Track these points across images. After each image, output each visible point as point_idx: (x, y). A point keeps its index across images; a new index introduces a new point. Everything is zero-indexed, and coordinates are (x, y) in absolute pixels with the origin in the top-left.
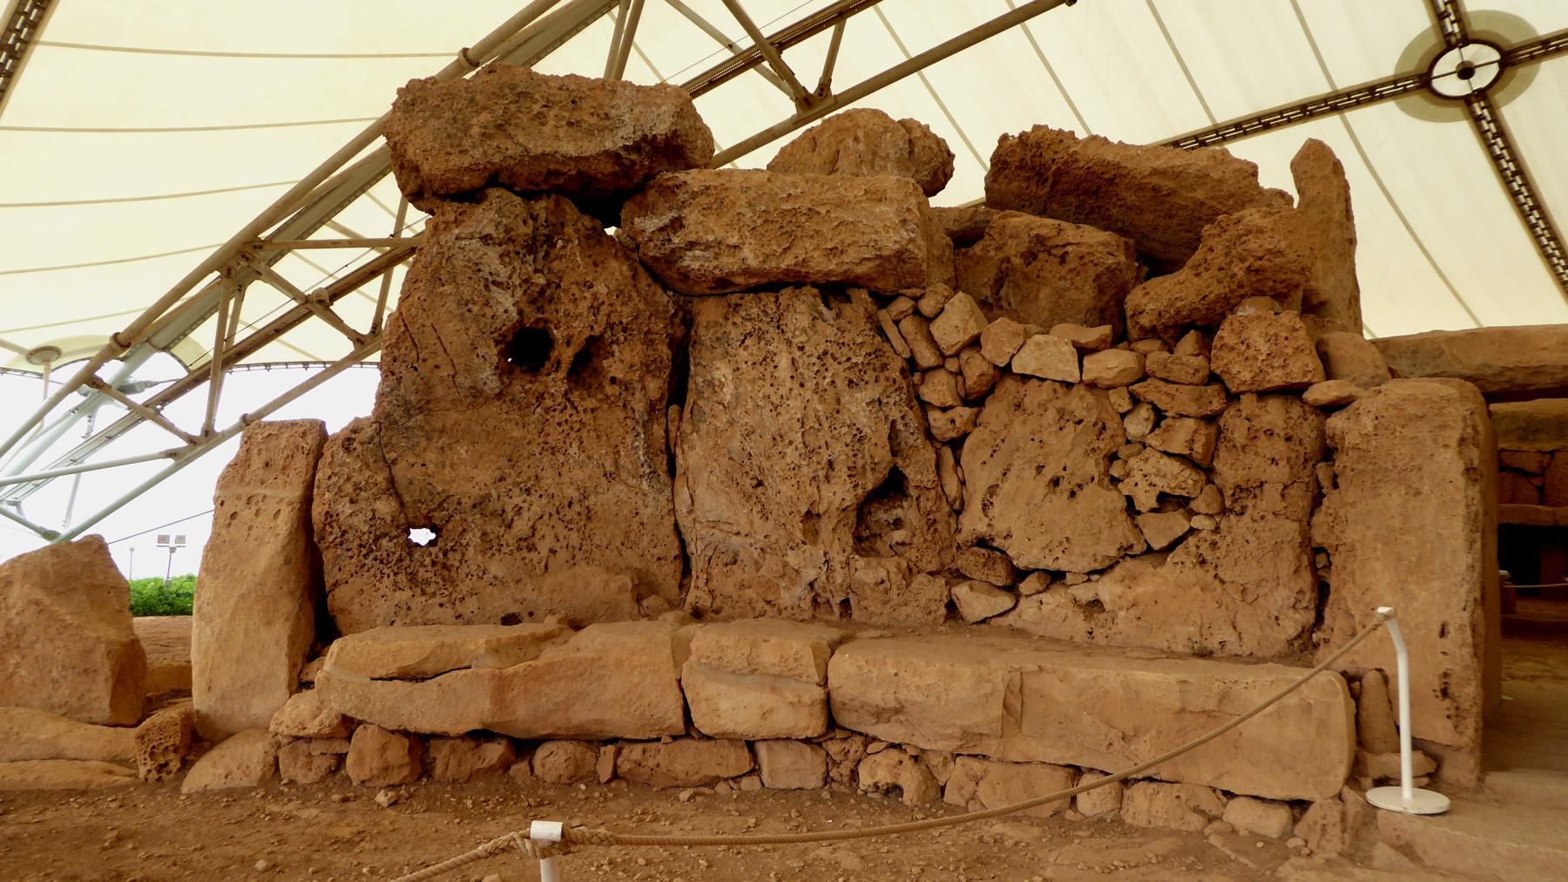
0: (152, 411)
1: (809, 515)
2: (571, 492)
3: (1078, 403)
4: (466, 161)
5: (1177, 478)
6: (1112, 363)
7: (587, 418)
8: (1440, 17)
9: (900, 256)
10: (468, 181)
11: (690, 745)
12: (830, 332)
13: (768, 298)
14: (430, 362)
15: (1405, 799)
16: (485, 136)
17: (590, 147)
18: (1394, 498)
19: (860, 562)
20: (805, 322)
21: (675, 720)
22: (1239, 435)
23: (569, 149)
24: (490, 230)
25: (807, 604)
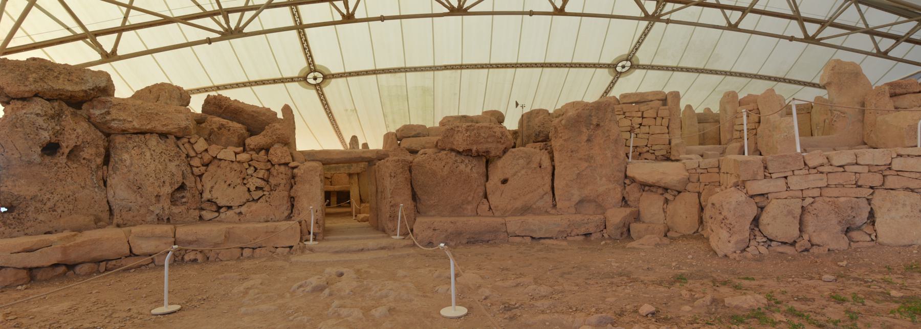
1: (158, 196)
2: (69, 193)
3: (235, 166)
4: (27, 89)
5: (260, 183)
6: (244, 157)
7: (74, 170)
8: (309, 64)
9: (186, 128)
10: (26, 95)
11: (132, 258)
12: (163, 147)
13: (142, 136)
14: (10, 153)
15: (311, 243)
16: (35, 81)
17: (77, 88)
18: (307, 186)
19: (174, 208)
20: (155, 143)
21: (128, 252)
22: (275, 174)
23: (70, 88)
24: (39, 112)
25: (156, 220)
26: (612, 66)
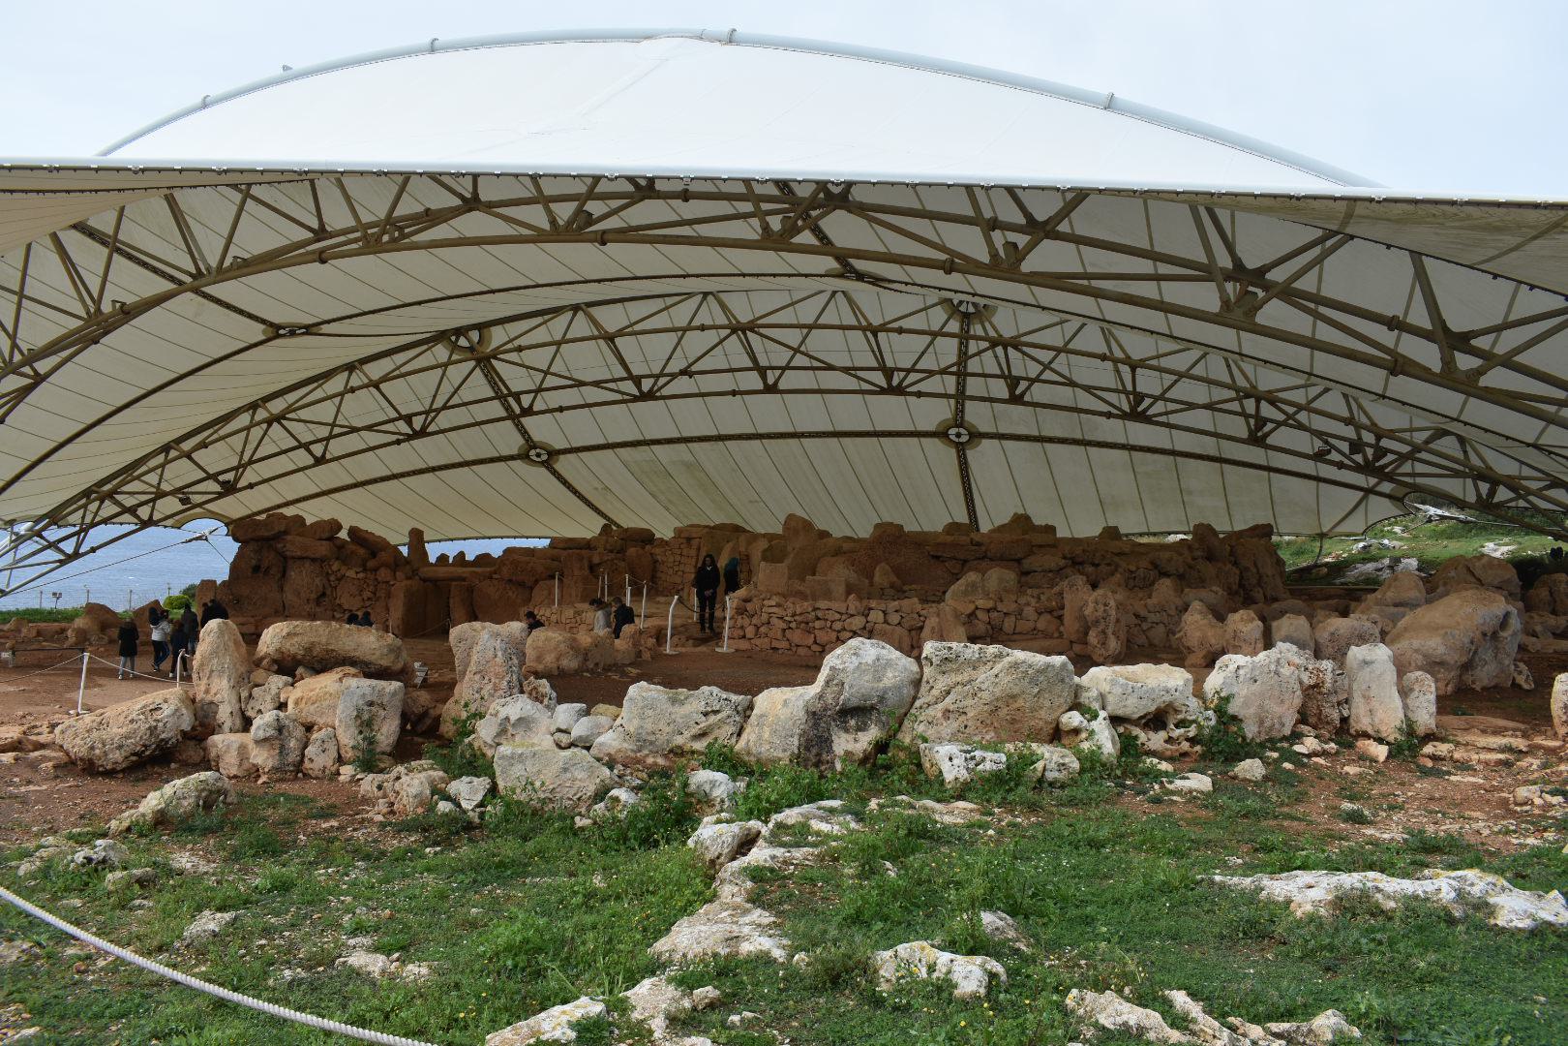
0: (53, 545)
26: (941, 434)
